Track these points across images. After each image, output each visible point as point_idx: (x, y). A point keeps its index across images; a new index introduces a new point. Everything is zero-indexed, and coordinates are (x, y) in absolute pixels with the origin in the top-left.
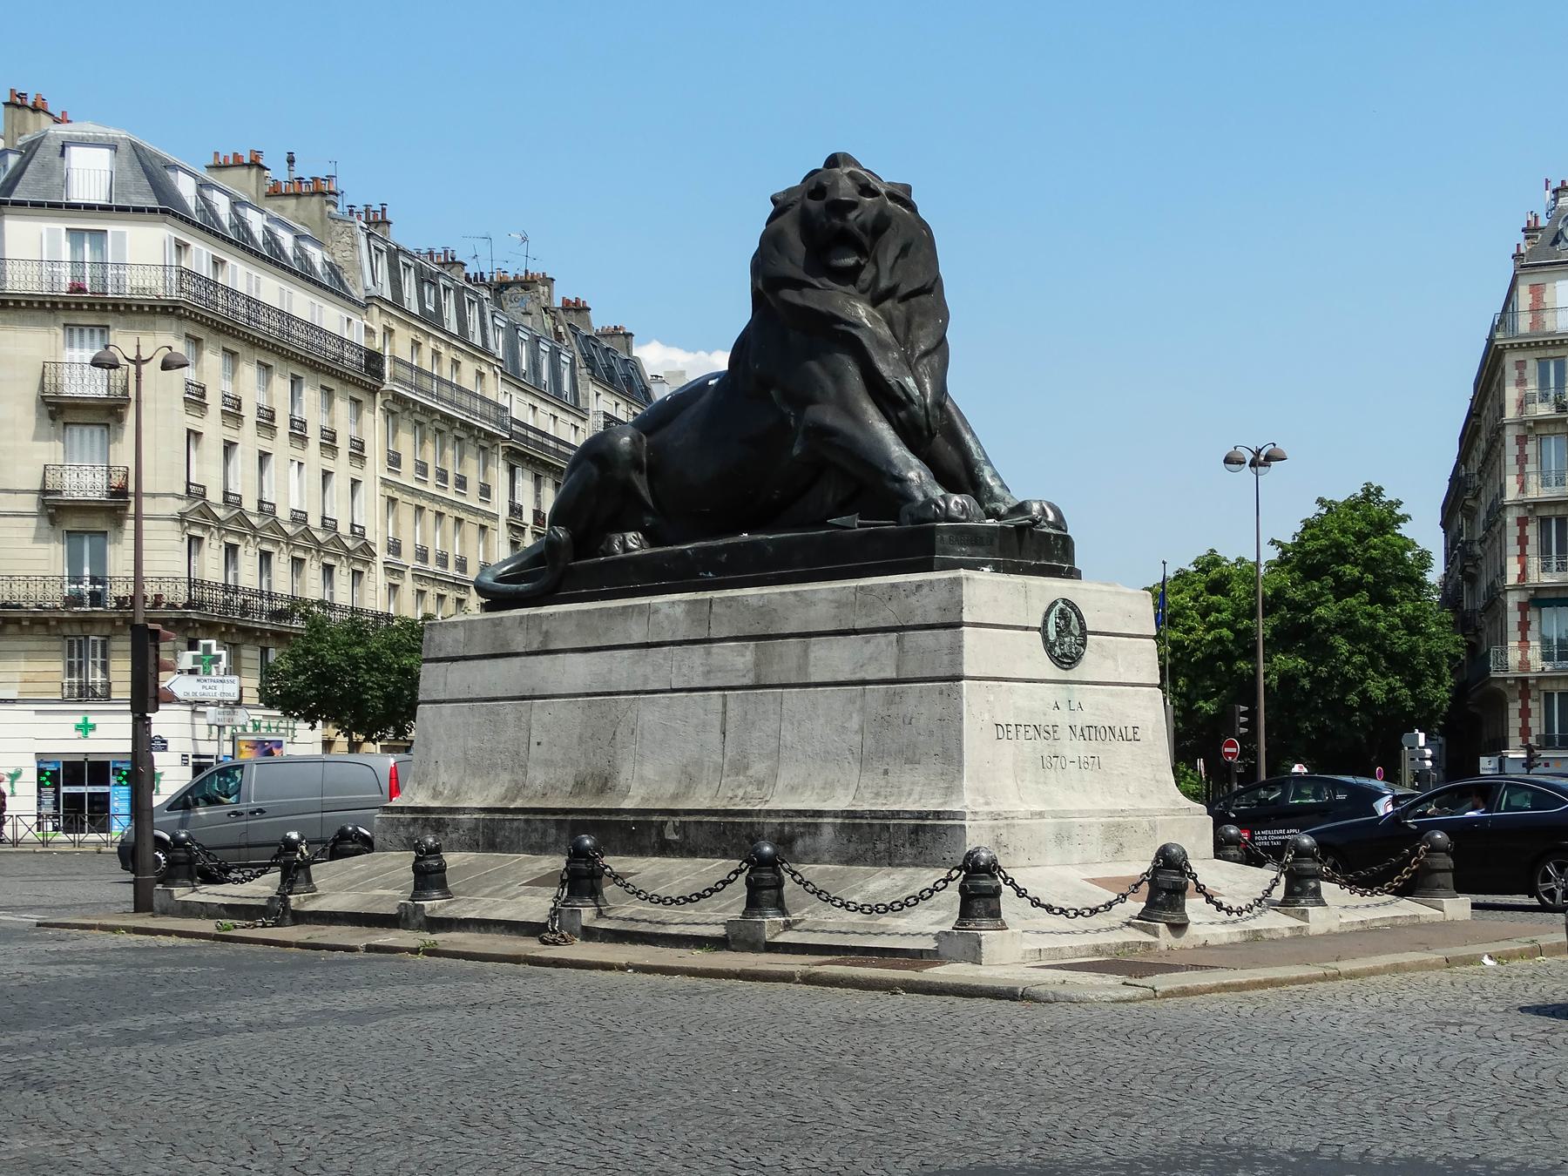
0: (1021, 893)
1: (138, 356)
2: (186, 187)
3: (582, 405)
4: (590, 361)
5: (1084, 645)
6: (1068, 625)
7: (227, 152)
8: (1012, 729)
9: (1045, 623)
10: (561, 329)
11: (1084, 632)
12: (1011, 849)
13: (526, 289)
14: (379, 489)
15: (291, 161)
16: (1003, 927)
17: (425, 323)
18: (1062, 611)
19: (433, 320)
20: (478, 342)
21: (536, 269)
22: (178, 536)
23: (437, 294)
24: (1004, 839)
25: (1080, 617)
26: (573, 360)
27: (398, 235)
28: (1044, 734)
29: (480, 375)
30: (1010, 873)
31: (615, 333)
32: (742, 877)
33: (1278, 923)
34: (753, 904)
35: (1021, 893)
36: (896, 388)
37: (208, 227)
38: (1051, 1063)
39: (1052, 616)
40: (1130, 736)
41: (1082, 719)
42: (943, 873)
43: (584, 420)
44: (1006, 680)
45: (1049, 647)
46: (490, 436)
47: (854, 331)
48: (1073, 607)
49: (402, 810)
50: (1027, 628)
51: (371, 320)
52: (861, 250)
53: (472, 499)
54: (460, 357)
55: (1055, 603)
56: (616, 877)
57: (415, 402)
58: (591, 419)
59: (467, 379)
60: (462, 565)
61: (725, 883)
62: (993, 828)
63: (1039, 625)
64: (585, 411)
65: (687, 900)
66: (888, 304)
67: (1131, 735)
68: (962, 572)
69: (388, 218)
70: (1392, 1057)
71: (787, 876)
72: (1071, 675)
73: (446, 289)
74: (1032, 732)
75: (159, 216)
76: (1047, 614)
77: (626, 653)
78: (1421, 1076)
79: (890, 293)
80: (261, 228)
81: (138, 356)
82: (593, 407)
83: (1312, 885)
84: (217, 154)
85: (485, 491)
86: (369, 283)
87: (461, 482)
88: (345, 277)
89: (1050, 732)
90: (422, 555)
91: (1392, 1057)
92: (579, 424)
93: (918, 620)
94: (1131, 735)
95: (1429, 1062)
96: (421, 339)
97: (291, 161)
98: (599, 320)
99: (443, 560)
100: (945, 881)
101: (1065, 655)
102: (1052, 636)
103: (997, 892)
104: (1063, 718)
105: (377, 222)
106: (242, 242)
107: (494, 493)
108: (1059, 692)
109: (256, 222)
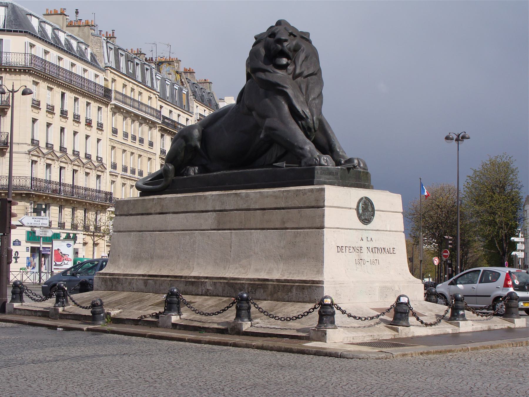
0: (344, 312)
1: (13, 89)
2: (35, 23)
3: (191, 111)
4: (194, 94)
5: (373, 215)
7: (51, 9)
8: (344, 248)
10: (183, 80)
13: (170, 64)
14: (109, 143)
15: (77, 12)
16: (336, 328)
17: (129, 77)
18: (365, 203)
19: (132, 76)
20: (149, 85)
21: (173, 56)
22: (27, 160)
23: (134, 66)
25: (372, 204)
26: (188, 93)
27: (118, 42)
28: (356, 251)
29: (150, 98)
30: (339, 305)
31: (205, 82)
32: (235, 305)
33: (446, 328)
34: (238, 316)
35: (344, 312)
36: (301, 112)
37: (43, 38)
38: (345, 384)
39: (361, 204)
40: (392, 252)
41: (371, 245)
42: (312, 305)
43: (191, 116)
44: (342, 229)
45: (360, 216)
46: (154, 123)
47: (285, 90)
49: (106, 274)
50: (351, 208)
51: (107, 76)
52: (288, 58)
53: (146, 146)
54: (142, 91)
55: (362, 198)
56: (187, 304)
57: (124, 109)
58: (194, 116)
59: (145, 100)
60: (141, 173)
61: (228, 307)
63: (355, 207)
64: (192, 113)
65: (213, 314)
66: (299, 79)
67: (391, 251)
68: (326, 187)
69: (115, 36)
70: (479, 384)
71: (252, 305)
73: (137, 64)
74: (352, 249)
75: (23, 34)
76: (359, 203)
77: (194, 214)
78: (489, 392)
79: (300, 75)
80: (64, 39)
81: (13, 89)
82: (195, 111)
83: (461, 312)
84: (47, 10)
85: (151, 144)
86: (107, 61)
87: (141, 141)
88: (97, 58)
89: (360, 250)
90: (125, 169)
91: (479, 384)
92: (189, 117)
93: (307, 204)
94: (391, 251)
95: (493, 386)
96: (127, 83)
97: (77, 12)
98: (198, 77)
99: (133, 172)
100: (313, 309)
101: (366, 219)
102: (361, 211)
103: (333, 314)
104: (364, 244)
105: (110, 38)
106: (56, 44)
107: (154, 145)
108: (365, 234)
109: (62, 37)
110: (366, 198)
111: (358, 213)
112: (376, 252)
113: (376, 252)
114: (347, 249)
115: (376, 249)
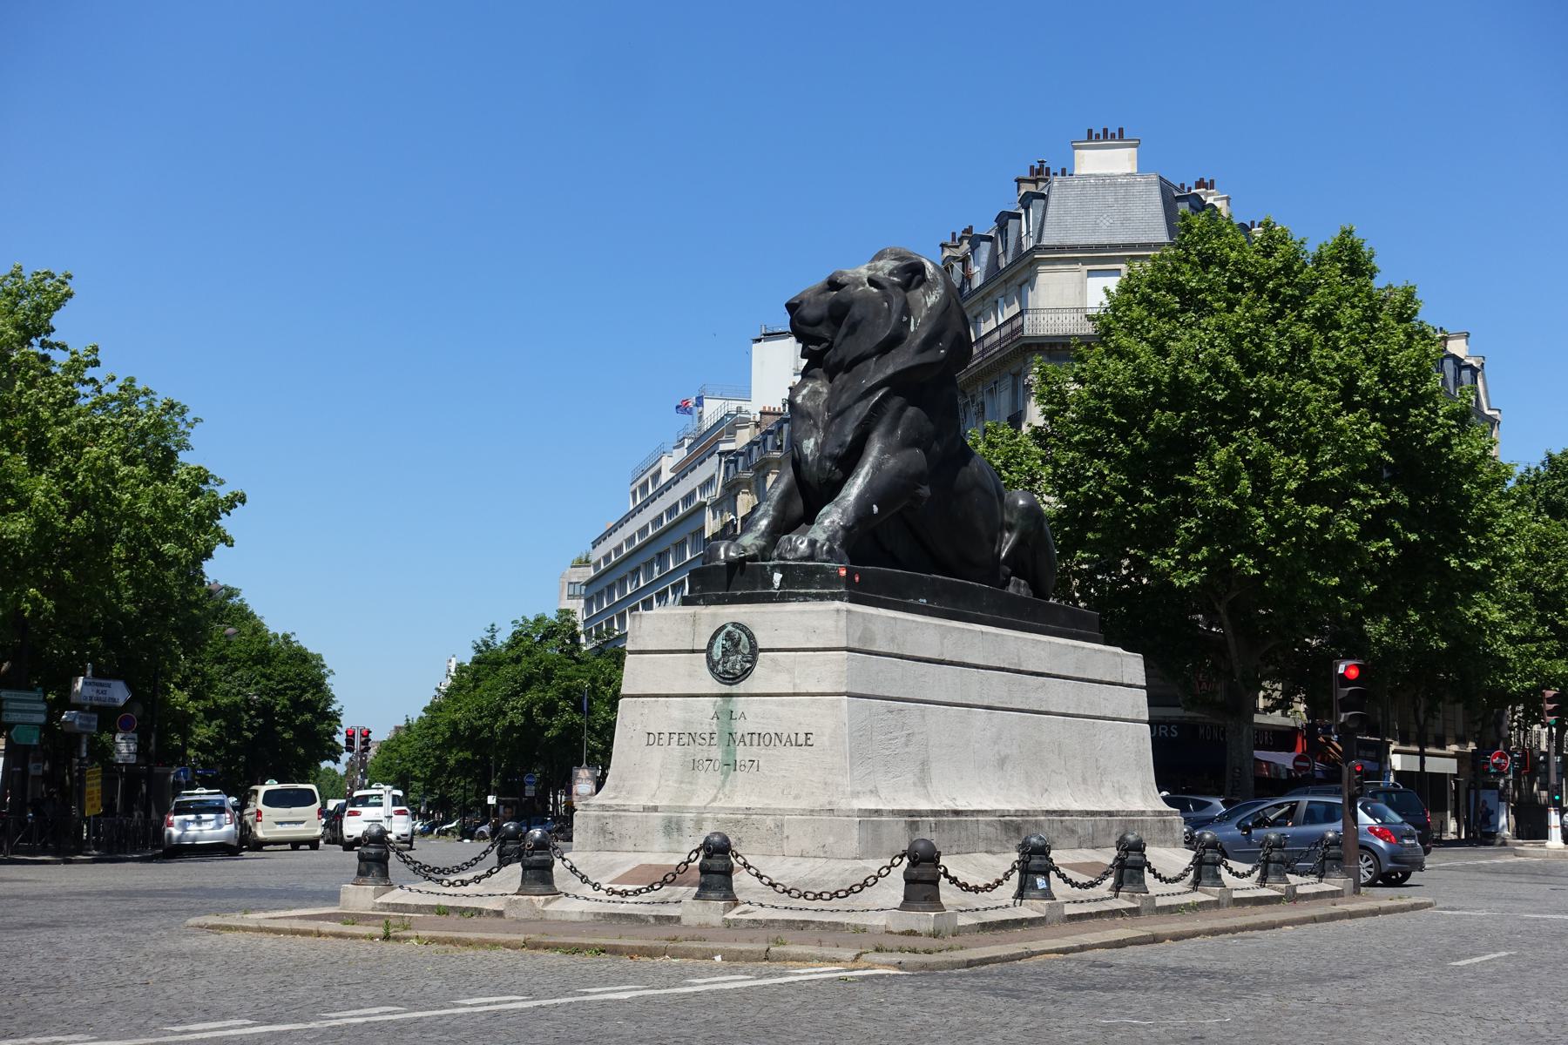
5: (753, 661)
6: (736, 645)
8: (665, 737)
9: (711, 645)
11: (755, 650)
12: (616, 836)
18: (729, 636)
24: (610, 827)
25: (751, 637)
39: (720, 640)
45: (712, 665)
48: (743, 628)
55: (724, 627)
62: (598, 818)
72: (734, 689)
74: (685, 739)
76: (714, 637)
101: (727, 672)
102: (717, 652)
110: (734, 624)
111: (709, 658)
112: (755, 742)
113: (755, 742)
114: (676, 737)
115: (755, 737)
